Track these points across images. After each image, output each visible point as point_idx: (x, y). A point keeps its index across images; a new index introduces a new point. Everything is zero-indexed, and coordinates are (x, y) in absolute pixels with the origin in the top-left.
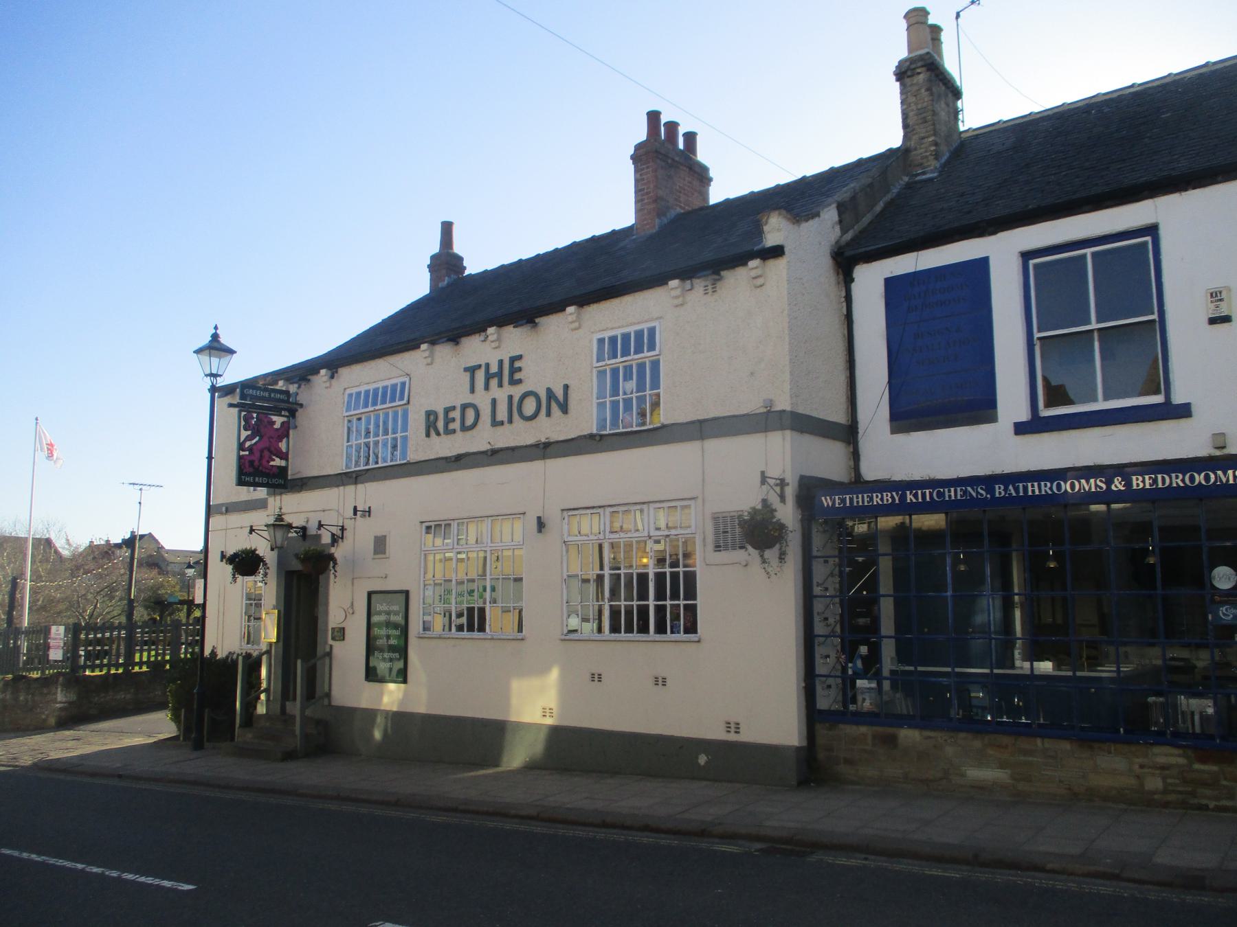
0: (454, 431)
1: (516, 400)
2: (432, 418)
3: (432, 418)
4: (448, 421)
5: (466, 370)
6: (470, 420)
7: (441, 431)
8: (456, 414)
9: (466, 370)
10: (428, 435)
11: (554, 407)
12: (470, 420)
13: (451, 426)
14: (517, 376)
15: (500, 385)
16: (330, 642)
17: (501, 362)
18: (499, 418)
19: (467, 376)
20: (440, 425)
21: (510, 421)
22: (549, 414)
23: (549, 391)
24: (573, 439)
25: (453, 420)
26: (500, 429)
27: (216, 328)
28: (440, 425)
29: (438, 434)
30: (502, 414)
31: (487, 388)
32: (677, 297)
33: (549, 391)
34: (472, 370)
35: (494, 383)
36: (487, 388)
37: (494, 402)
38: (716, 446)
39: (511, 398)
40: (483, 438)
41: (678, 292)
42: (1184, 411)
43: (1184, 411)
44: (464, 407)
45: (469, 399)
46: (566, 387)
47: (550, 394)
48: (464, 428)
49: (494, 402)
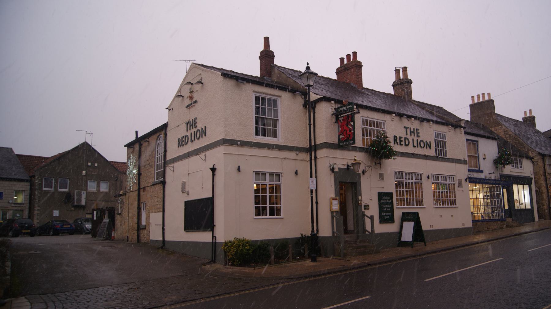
0: (402, 145)
1: (419, 141)
2: (396, 139)
3: (396, 139)
4: (401, 141)
5: (405, 127)
6: (407, 143)
7: (399, 143)
8: (403, 139)
9: (405, 127)
10: (395, 143)
11: (428, 147)
12: (407, 143)
13: (402, 143)
14: (419, 135)
15: (414, 136)
16: (363, 210)
17: (414, 129)
18: (414, 145)
19: (405, 130)
20: (398, 141)
21: (418, 147)
22: (427, 148)
23: (426, 141)
24: (431, 156)
25: (402, 141)
26: (414, 149)
27: (308, 64)
28: (398, 141)
29: (398, 144)
30: (415, 144)
31: (411, 135)
32: (450, 130)
33: (426, 141)
34: (406, 128)
35: (412, 134)
36: (411, 135)
37: (413, 139)
38: (458, 165)
39: (417, 140)
40: (410, 150)
41: (450, 129)
42: (482, 172)
43: (482, 172)
44: (405, 138)
45: (406, 136)
46: (430, 142)
47: (427, 144)
48: (406, 145)
49: (413, 139)
